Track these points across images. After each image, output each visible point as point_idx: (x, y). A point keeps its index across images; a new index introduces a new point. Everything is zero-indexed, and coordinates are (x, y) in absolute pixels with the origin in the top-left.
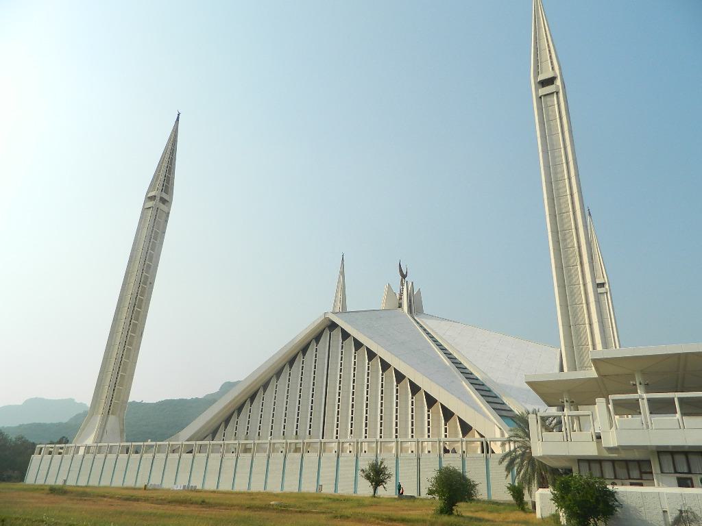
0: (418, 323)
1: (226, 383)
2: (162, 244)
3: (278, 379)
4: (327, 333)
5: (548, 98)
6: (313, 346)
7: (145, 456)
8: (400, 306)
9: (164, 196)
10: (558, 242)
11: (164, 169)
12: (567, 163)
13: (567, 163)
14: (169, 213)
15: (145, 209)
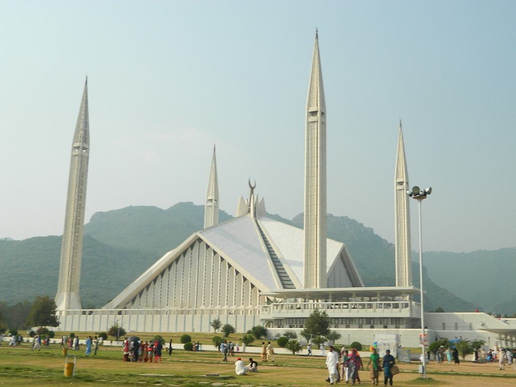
0: (258, 226)
1: (97, 214)
2: (86, 179)
3: (169, 270)
4: (197, 244)
5: (313, 124)
6: (189, 251)
7: (96, 316)
8: (249, 211)
9: (85, 146)
10: (308, 211)
11: (82, 126)
12: (317, 167)
13: (317, 167)
14: (88, 157)
15: (73, 156)
